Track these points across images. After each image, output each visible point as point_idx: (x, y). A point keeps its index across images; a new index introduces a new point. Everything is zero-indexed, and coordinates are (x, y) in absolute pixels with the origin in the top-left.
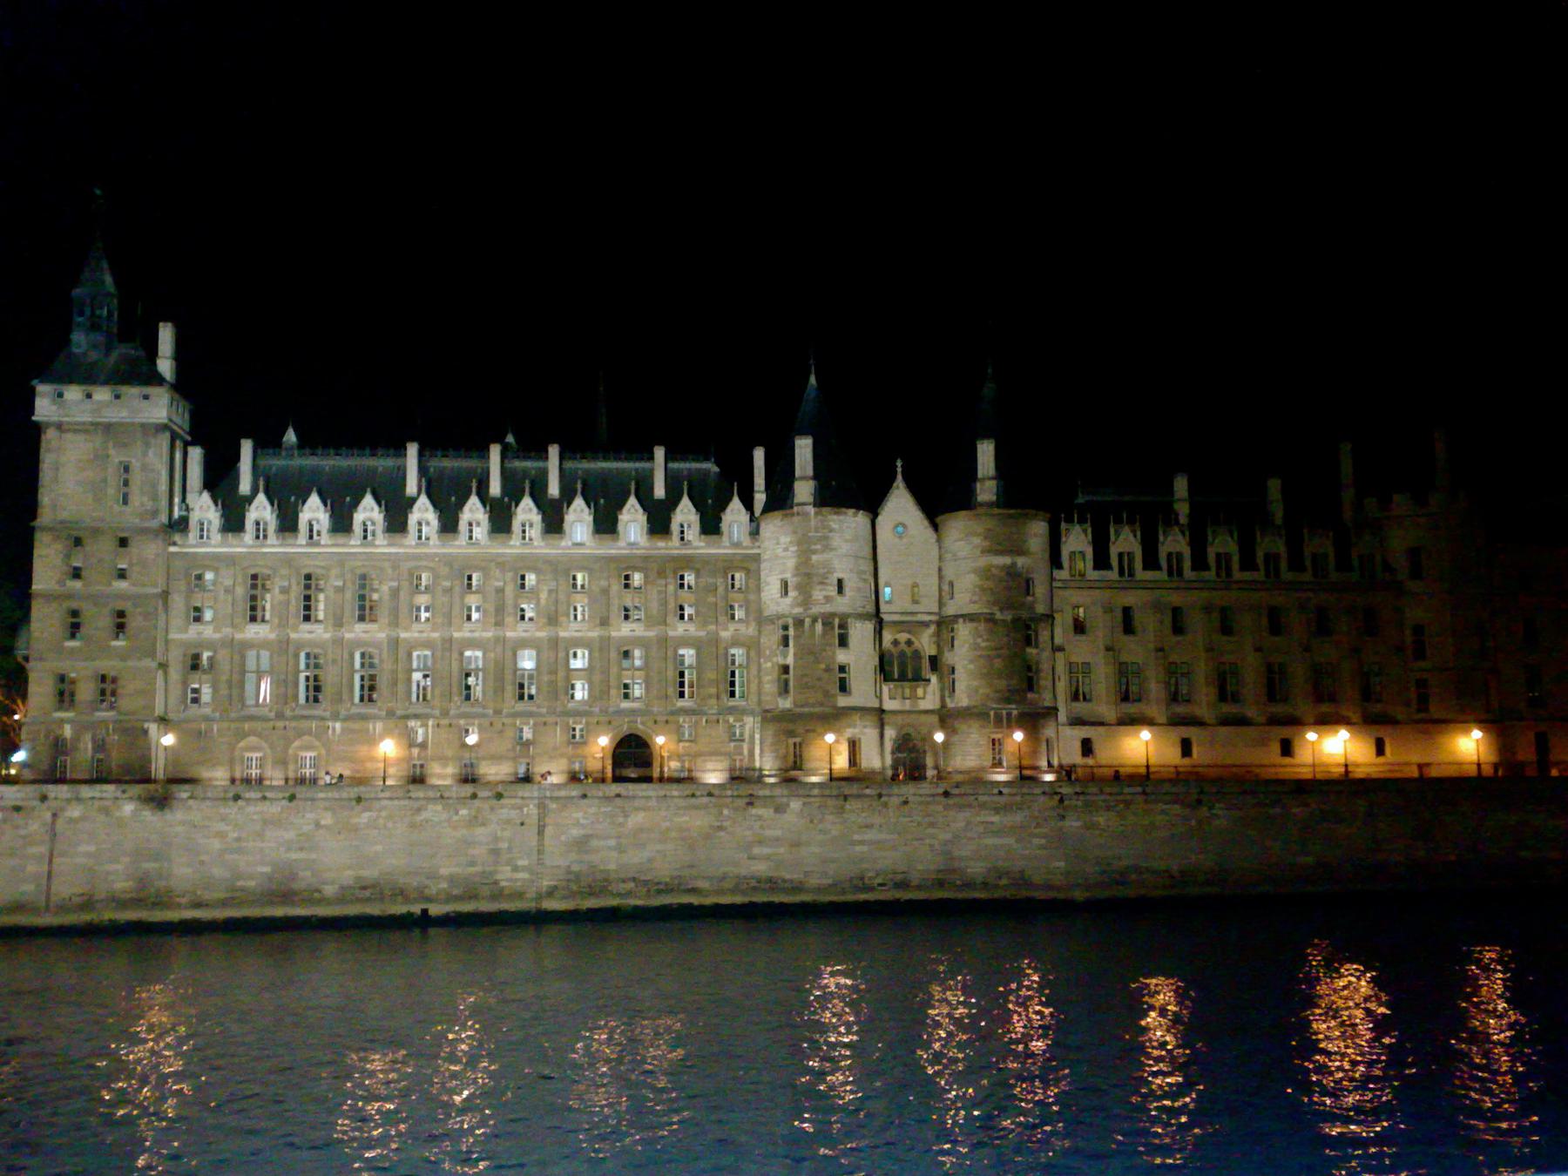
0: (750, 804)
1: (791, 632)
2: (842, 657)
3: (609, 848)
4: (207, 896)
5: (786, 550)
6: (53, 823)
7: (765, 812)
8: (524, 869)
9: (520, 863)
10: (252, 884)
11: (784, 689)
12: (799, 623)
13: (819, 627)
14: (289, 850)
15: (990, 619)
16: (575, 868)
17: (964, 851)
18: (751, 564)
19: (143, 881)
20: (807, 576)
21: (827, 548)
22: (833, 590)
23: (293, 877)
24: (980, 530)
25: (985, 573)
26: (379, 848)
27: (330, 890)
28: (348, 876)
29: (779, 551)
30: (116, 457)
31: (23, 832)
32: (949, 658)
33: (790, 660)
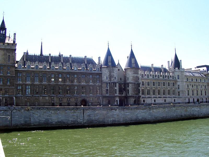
0: (112, 110)
1: (108, 84)
2: (115, 89)
3: (93, 116)
4: (35, 124)
5: (107, 72)
6: (11, 113)
7: (114, 111)
8: (82, 119)
9: (81, 118)
10: (42, 122)
11: (107, 93)
12: (109, 83)
13: (112, 84)
14: (47, 117)
15: (134, 83)
16: (88, 119)
17: (139, 115)
18: (100, 75)
19: (26, 122)
20: (111, 77)
21: (113, 72)
22: (114, 79)
23: (49, 121)
24: (133, 70)
25: (133, 77)
26: (61, 116)
27: (54, 123)
28: (56, 121)
29: (106, 73)
30: (8, 54)
31: (7, 114)
32: (128, 88)
33: (108, 88)
